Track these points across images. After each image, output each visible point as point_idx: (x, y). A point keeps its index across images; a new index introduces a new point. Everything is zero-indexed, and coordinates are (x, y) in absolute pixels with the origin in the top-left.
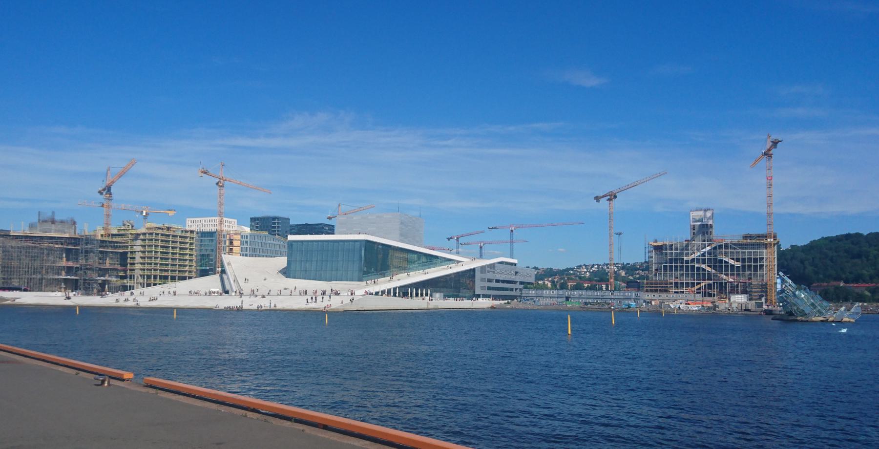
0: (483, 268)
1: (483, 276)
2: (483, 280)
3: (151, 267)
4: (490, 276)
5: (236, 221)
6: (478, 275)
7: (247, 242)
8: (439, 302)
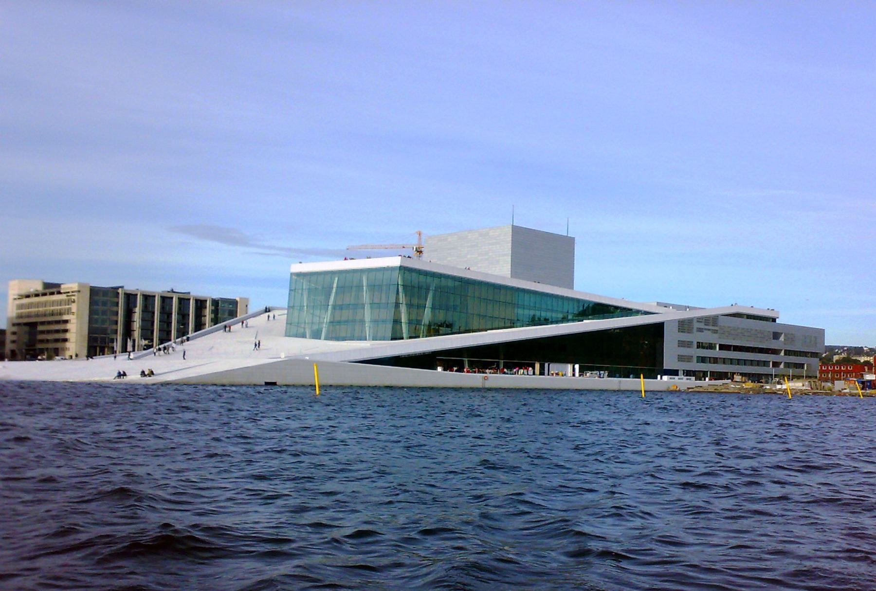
1: (685, 337)
2: (682, 344)
4: (707, 337)
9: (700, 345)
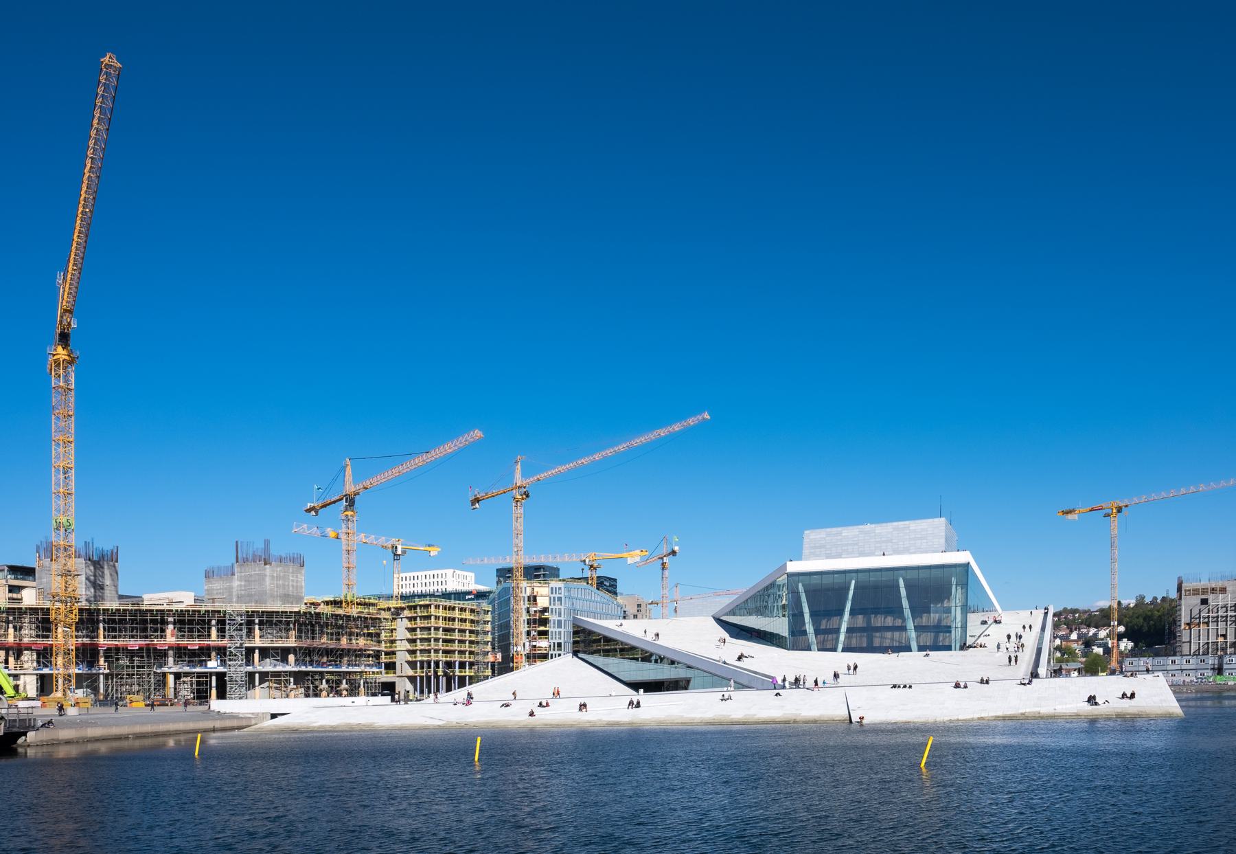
3: (430, 645)
5: (473, 575)
7: (560, 599)
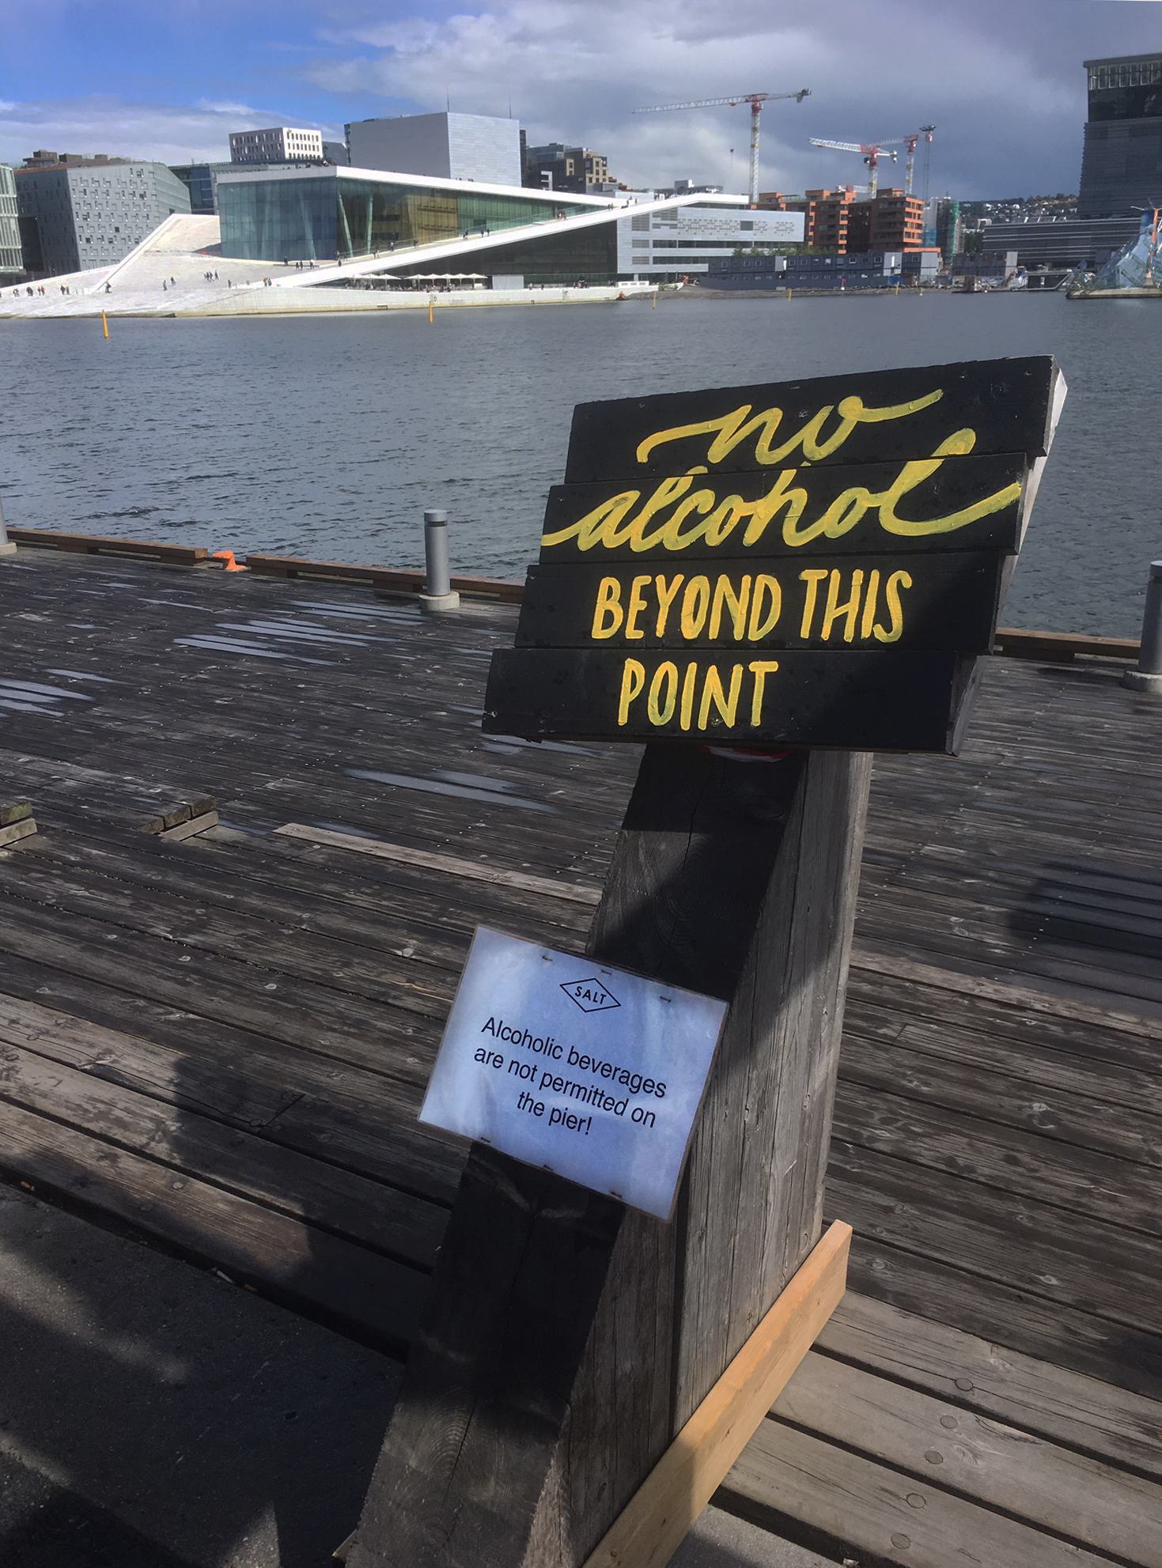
0: (640, 222)
2: (637, 244)
6: (624, 237)
8: (510, 292)
9: (658, 244)
